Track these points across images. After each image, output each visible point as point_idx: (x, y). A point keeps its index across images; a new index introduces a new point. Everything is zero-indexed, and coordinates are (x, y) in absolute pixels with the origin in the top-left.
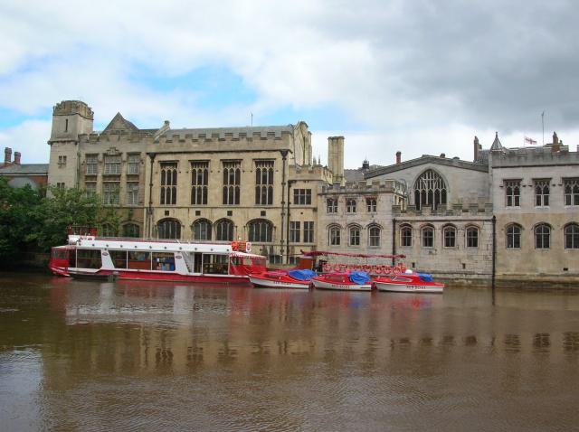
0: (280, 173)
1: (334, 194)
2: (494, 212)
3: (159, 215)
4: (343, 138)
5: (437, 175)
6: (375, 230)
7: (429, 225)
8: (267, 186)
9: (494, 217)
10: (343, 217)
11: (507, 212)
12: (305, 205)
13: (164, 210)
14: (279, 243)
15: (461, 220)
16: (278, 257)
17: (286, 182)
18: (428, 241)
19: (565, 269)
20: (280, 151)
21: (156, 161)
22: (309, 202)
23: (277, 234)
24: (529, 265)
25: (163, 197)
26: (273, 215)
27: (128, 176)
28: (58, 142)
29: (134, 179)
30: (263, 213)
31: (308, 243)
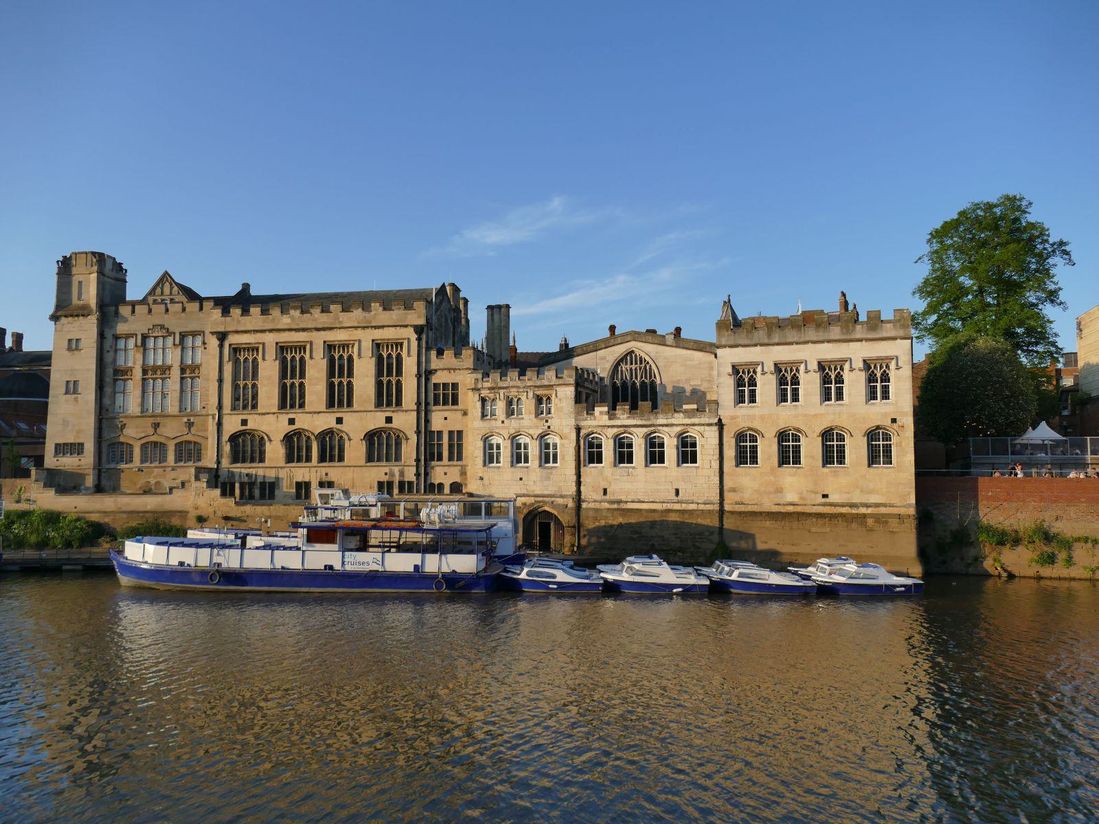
3: (232, 425)
4: (508, 307)
8: (394, 380)
9: (720, 420)
12: (450, 407)
16: (410, 483)
22: (455, 402)
25: (236, 399)
29: (189, 371)
30: (389, 420)
31: (455, 463)
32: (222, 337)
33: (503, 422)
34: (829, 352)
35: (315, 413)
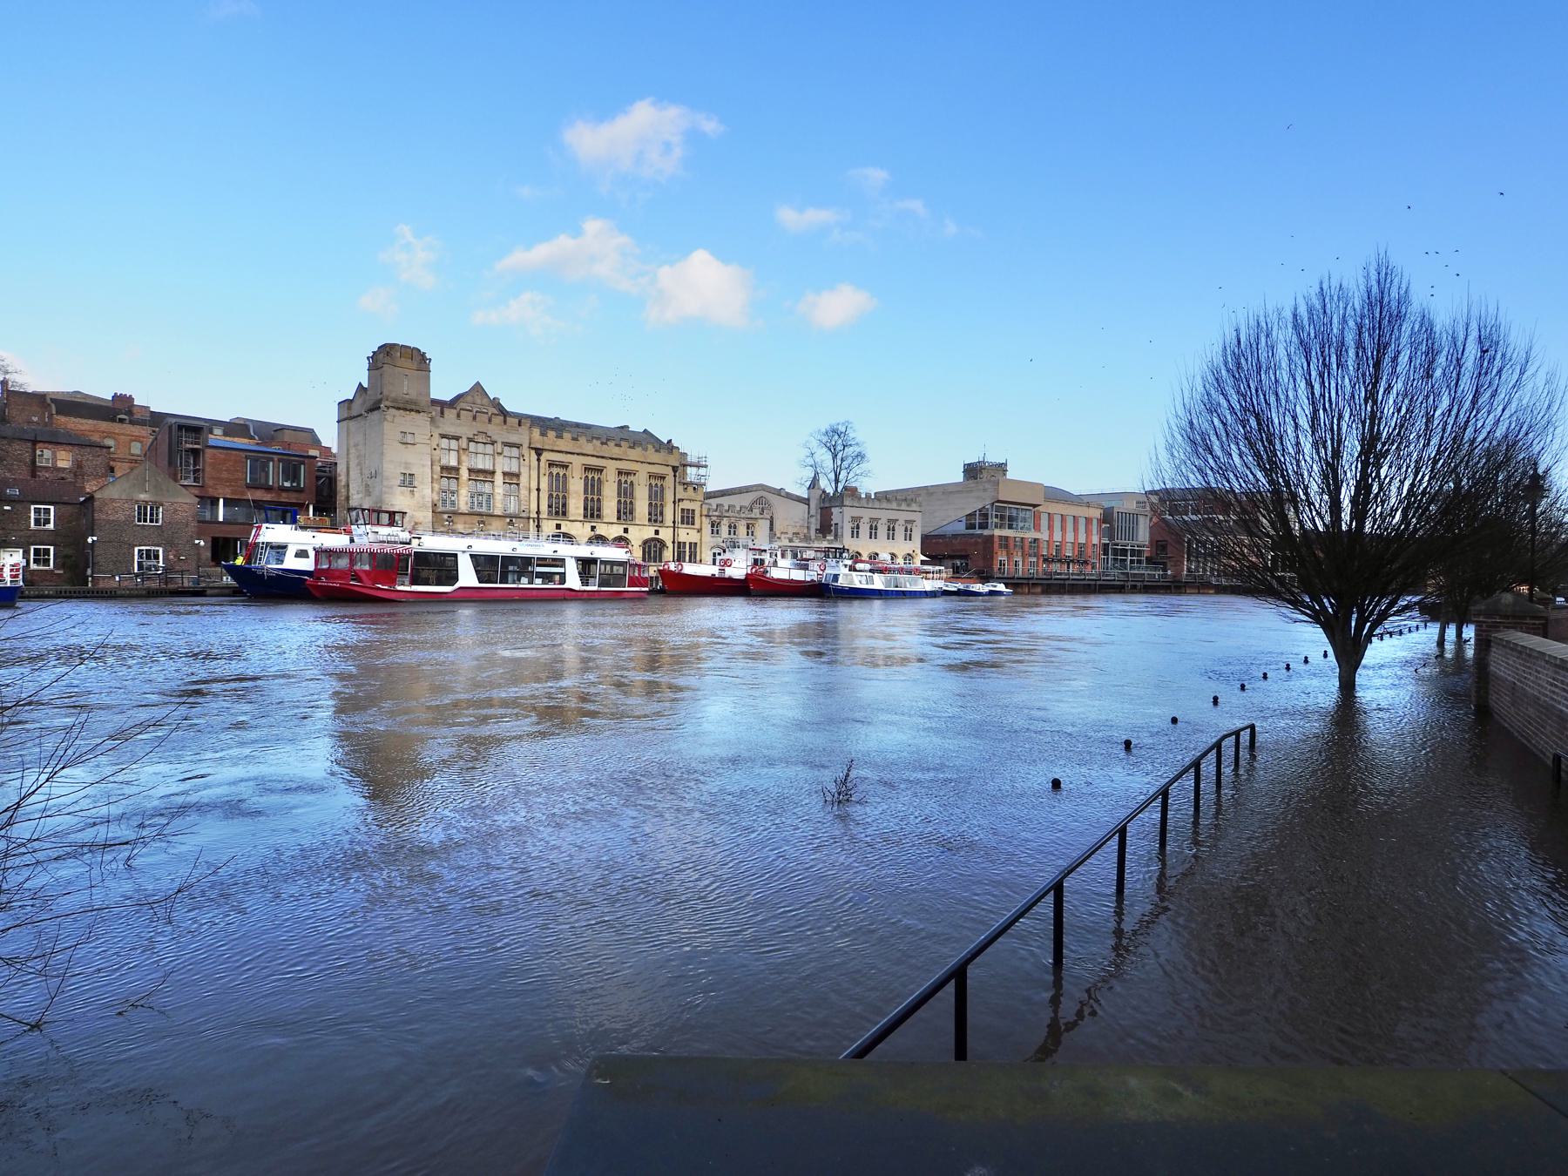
2: (844, 542)
12: (690, 526)
22: (693, 524)
25: (550, 506)
26: (666, 535)
27: (505, 474)
28: (399, 409)
30: (657, 532)
34: (893, 515)
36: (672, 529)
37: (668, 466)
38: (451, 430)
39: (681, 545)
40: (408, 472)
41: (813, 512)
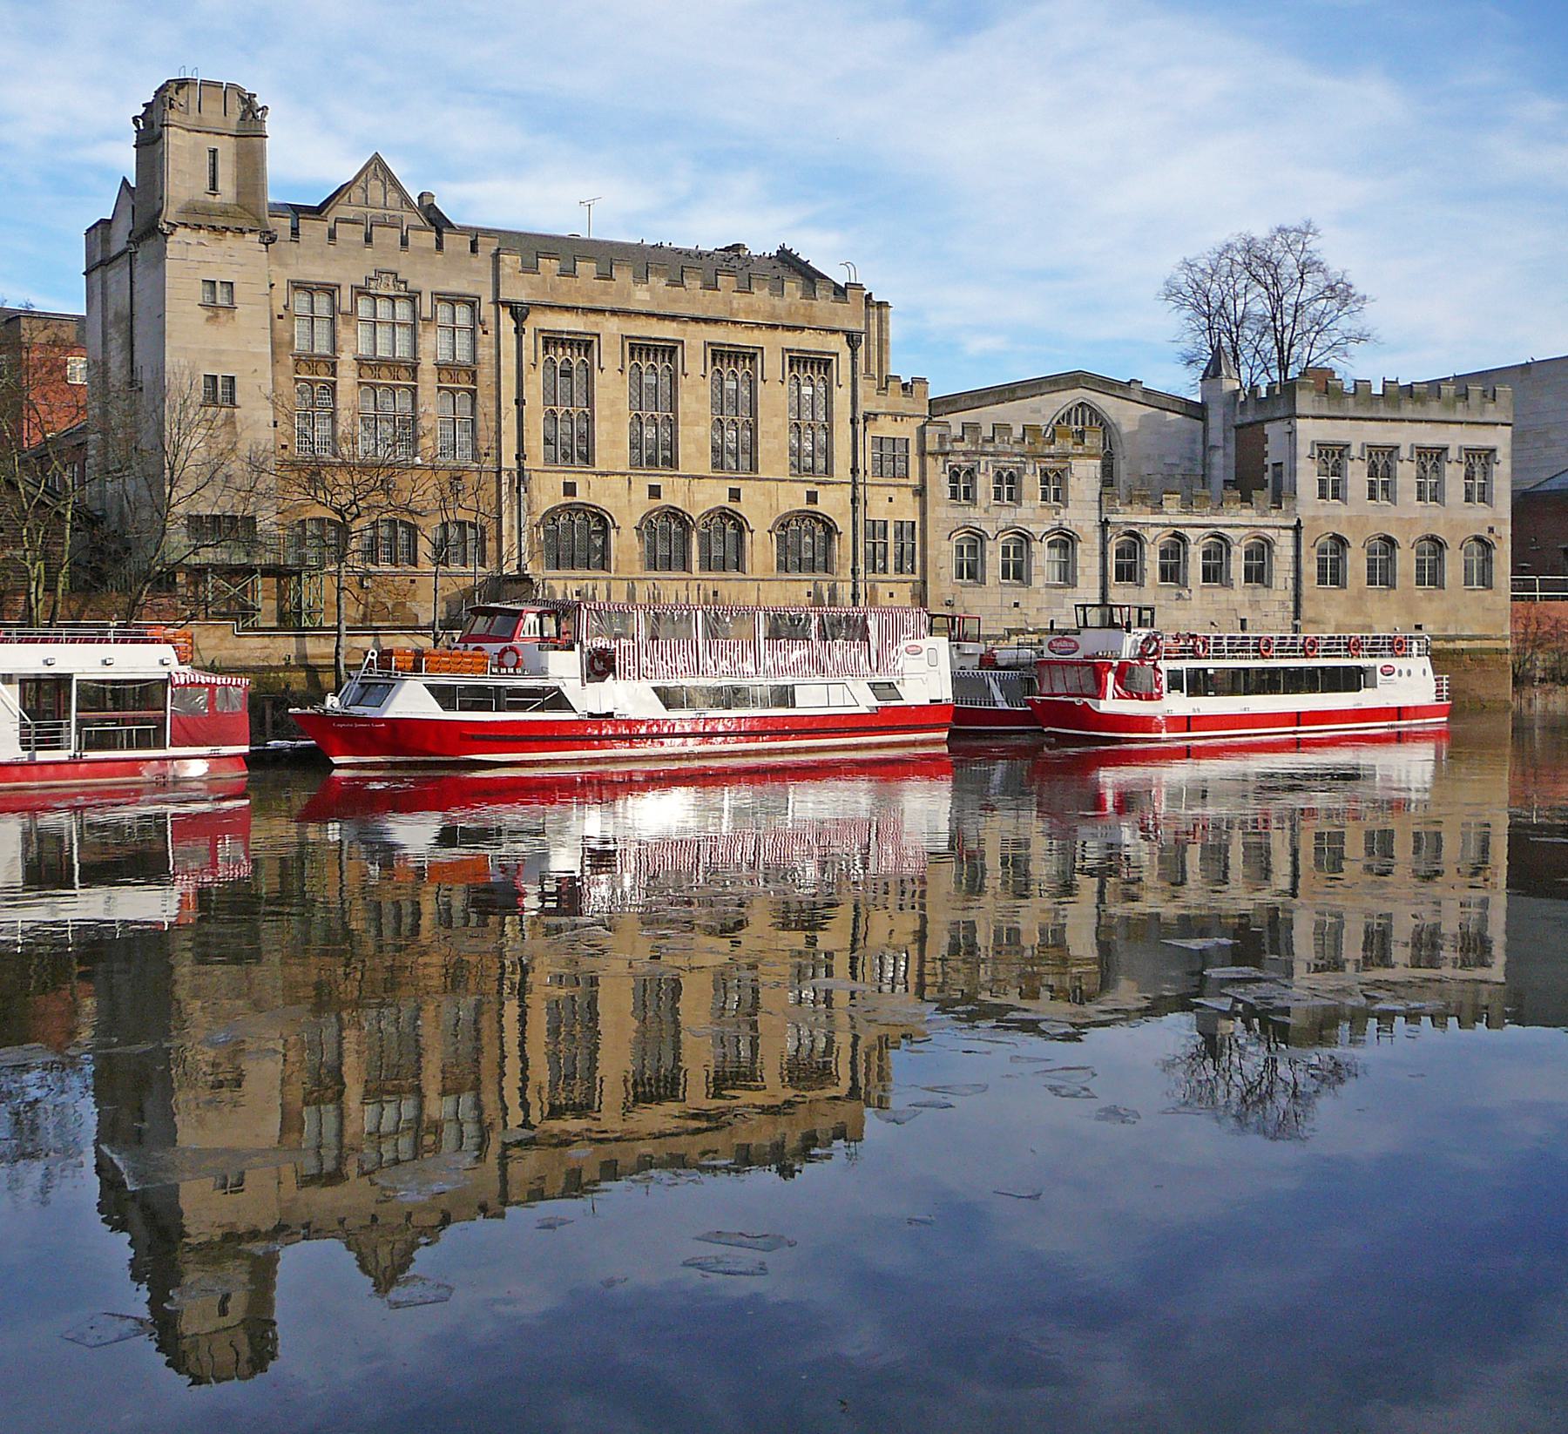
0: (847, 390)
1: (965, 454)
2: (1298, 510)
3: (547, 492)
5: (1096, 415)
6: (1065, 541)
7: (1175, 535)
9: (1299, 521)
10: (988, 515)
11: (1322, 512)
13: (561, 478)
14: (850, 576)
15: (1238, 526)
17: (860, 417)
18: (1172, 573)
19: (1419, 627)
20: (843, 331)
21: (529, 328)
23: (842, 549)
24: (1358, 620)
26: (833, 502)
30: (812, 497)
31: (904, 577)
32: (519, 313)
33: (986, 511)
35: (694, 477)
36: (850, 487)
37: (837, 331)
38: (316, 272)
39: (876, 530)
40: (219, 373)
41: (1216, 437)
